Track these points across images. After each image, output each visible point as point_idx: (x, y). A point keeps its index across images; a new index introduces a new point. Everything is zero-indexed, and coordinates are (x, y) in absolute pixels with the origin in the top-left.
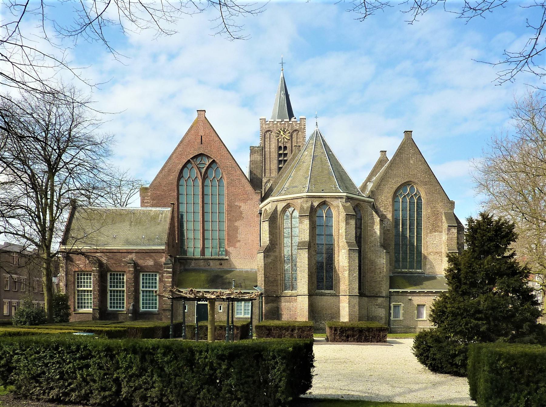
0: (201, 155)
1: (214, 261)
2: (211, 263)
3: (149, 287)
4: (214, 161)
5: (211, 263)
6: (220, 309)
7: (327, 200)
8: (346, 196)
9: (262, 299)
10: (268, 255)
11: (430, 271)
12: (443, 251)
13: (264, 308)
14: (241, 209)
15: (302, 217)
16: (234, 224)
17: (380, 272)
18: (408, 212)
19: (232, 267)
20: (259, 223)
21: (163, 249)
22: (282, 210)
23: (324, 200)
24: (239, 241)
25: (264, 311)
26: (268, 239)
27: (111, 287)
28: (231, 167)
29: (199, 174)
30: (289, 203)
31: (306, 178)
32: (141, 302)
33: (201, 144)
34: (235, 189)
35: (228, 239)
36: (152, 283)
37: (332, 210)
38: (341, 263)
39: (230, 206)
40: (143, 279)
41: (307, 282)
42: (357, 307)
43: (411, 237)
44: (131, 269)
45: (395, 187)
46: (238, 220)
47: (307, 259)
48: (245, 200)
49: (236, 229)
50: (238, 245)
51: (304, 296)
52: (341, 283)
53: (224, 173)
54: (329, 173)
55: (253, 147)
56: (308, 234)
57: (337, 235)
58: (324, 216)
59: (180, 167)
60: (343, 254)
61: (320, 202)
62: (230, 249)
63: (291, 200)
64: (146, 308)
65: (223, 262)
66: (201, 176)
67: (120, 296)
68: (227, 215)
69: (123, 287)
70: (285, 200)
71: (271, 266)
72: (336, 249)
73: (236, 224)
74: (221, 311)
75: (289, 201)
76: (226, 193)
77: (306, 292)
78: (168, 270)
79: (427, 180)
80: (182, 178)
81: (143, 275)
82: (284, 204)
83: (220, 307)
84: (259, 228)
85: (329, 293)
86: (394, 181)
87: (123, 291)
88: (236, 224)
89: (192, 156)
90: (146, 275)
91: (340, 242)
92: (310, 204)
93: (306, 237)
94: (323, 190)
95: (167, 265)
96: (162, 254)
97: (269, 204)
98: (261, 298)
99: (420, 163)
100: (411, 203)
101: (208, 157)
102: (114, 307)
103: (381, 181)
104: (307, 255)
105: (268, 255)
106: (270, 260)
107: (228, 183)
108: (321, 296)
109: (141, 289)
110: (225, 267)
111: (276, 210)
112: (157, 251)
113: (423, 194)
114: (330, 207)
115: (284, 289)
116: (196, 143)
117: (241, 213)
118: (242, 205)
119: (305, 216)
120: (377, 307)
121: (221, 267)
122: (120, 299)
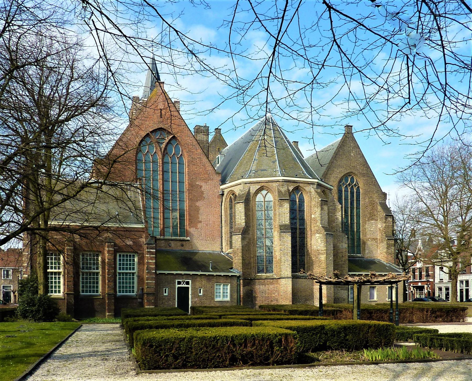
1: (175, 242)
2: (172, 244)
3: (127, 269)
4: (174, 137)
5: (173, 244)
6: (200, 293)
7: (301, 185)
8: (317, 182)
9: (240, 282)
10: (244, 237)
11: (368, 255)
12: (378, 237)
13: (242, 291)
14: (203, 189)
15: (282, 201)
16: (195, 204)
17: (343, 256)
18: (349, 201)
19: (194, 248)
20: (220, 204)
21: (143, 228)
22: (255, 192)
24: (201, 222)
25: (242, 294)
26: (244, 221)
27: (120, 269)
28: (192, 145)
30: (263, 186)
31: (274, 162)
33: (161, 118)
34: (196, 168)
35: (189, 219)
36: (130, 264)
37: (304, 196)
38: (315, 247)
39: (191, 185)
40: (120, 260)
41: (291, 265)
43: (352, 224)
44: (111, 249)
45: (340, 176)
47: (290, 242)
48: (206, 180)
49: (197, 210)
50: (199, 225)
51: (288, 279)
53: (184, 151)
54: (294, 159)
55: (200, 126)
56: (288, 218)
57: (309, 219)
58: (297, 200)
59: (138, 140)
60: (317, 238)
61: (294, 187)
62: (192, 230)
65: (184, 243)
66: (161, 151)
67: (94, 278)
68: (189, 194)
69: (97, 269)
70: (259, 183)
71: (246, 249)
72: (309, 233)
73: (198, 204)
74: (166, 294)
75: (263, 184)
76: (187, 171)
78: (152, 250)
79: (365, 172)
80: (140, 152)
81: (120, 256)
82: (258, 187)
83: (200, 290)
84: (220, 209)
85: (303, 276)
86: (338, 171)
87: (97, 274)
88: (198, 204)
89: (151, 130)
90: (124, 256)
91: (312, 226)
92: (286, 188)
93: (286, 220)
94: (296, 176)
97: (240, 185)
98: (239, 281)
99: (359, 156)
100: (352, 193)
101: (169, 133)
102: (87, 292)
103: (328, 171)
104: (290, 238)
105: (244, 237)
106: (246, 243)
107: (188, 162)
108: (297, 278)
109: (118, 271)
110: (187, 248)
111: (249, 192)
112: (136, 230)
113: (361, 185)
114: (302, 192)
115: (257, 272)
116: (155, 116)
117: (202, 192)
118: (203, 184)
119: (285, 199)
120: (340, 289)
121: (183, 248)
122: (123, 283)
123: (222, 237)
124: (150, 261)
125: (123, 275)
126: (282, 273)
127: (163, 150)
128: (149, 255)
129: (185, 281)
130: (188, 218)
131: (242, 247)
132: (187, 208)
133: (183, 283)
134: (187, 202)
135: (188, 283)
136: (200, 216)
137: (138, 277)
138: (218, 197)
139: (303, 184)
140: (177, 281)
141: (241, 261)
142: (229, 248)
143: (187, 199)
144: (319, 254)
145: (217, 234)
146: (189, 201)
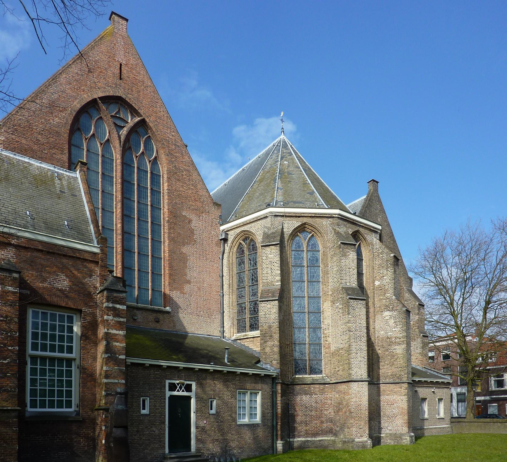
3: (53, 349)
14: (193, 224)
16: (180, 249)
24: (189, 282)
35: (171, 275)
39: (174, 214)
46: (187, 243)
48: (199, 212)
49: (184, 259)
50: (187, 288)
52: (381, 364)
62: (175, 295)
63: (310, 219)
64: (43, 405)
65: (161, 317)
68: (169, 229)
77: (365, 376)
78: (118, 306)
84: (221, 263)
95: (115, 295)
96: (92, 266)
110: (165, 327)
117: (192, 232)
118: (193, 217)
123: (223, 312)
124: (114, 332)
126: (353, 372)
128: (111, 318)
129: (183, 384)
130: (167, 272)
132: (167, 255)
133: (181, 388)
134: (166, 244)
135: (188, 388)
136: (187, 271)
137: (83, 370)
138: (217, 245)
140: (167, 382)
141: (276, 349)
142: (236, 331)
143: (166, 239)
144: (391, 343)
145: (215, 307)
146: (170, 242)
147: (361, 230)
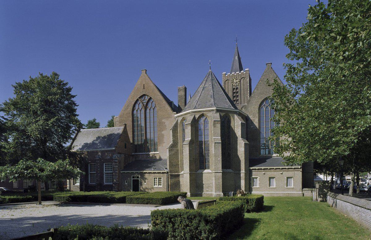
0: (144, 95)
6: (145, 182)
7: (204, 113)
22: (181, 122)
23: (202, 113)
29: (143, 106)
30: (183, 118)
32: (105, 179)
42: (221, 180)
81: (105, 164)
88: (163, 133)
106: (173, 152)
125: (107, 174)
127: (145, 106)
131: (169, 155)
139: (206, 112)
147: (204, 113)
